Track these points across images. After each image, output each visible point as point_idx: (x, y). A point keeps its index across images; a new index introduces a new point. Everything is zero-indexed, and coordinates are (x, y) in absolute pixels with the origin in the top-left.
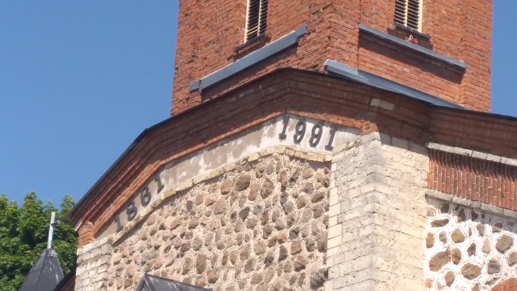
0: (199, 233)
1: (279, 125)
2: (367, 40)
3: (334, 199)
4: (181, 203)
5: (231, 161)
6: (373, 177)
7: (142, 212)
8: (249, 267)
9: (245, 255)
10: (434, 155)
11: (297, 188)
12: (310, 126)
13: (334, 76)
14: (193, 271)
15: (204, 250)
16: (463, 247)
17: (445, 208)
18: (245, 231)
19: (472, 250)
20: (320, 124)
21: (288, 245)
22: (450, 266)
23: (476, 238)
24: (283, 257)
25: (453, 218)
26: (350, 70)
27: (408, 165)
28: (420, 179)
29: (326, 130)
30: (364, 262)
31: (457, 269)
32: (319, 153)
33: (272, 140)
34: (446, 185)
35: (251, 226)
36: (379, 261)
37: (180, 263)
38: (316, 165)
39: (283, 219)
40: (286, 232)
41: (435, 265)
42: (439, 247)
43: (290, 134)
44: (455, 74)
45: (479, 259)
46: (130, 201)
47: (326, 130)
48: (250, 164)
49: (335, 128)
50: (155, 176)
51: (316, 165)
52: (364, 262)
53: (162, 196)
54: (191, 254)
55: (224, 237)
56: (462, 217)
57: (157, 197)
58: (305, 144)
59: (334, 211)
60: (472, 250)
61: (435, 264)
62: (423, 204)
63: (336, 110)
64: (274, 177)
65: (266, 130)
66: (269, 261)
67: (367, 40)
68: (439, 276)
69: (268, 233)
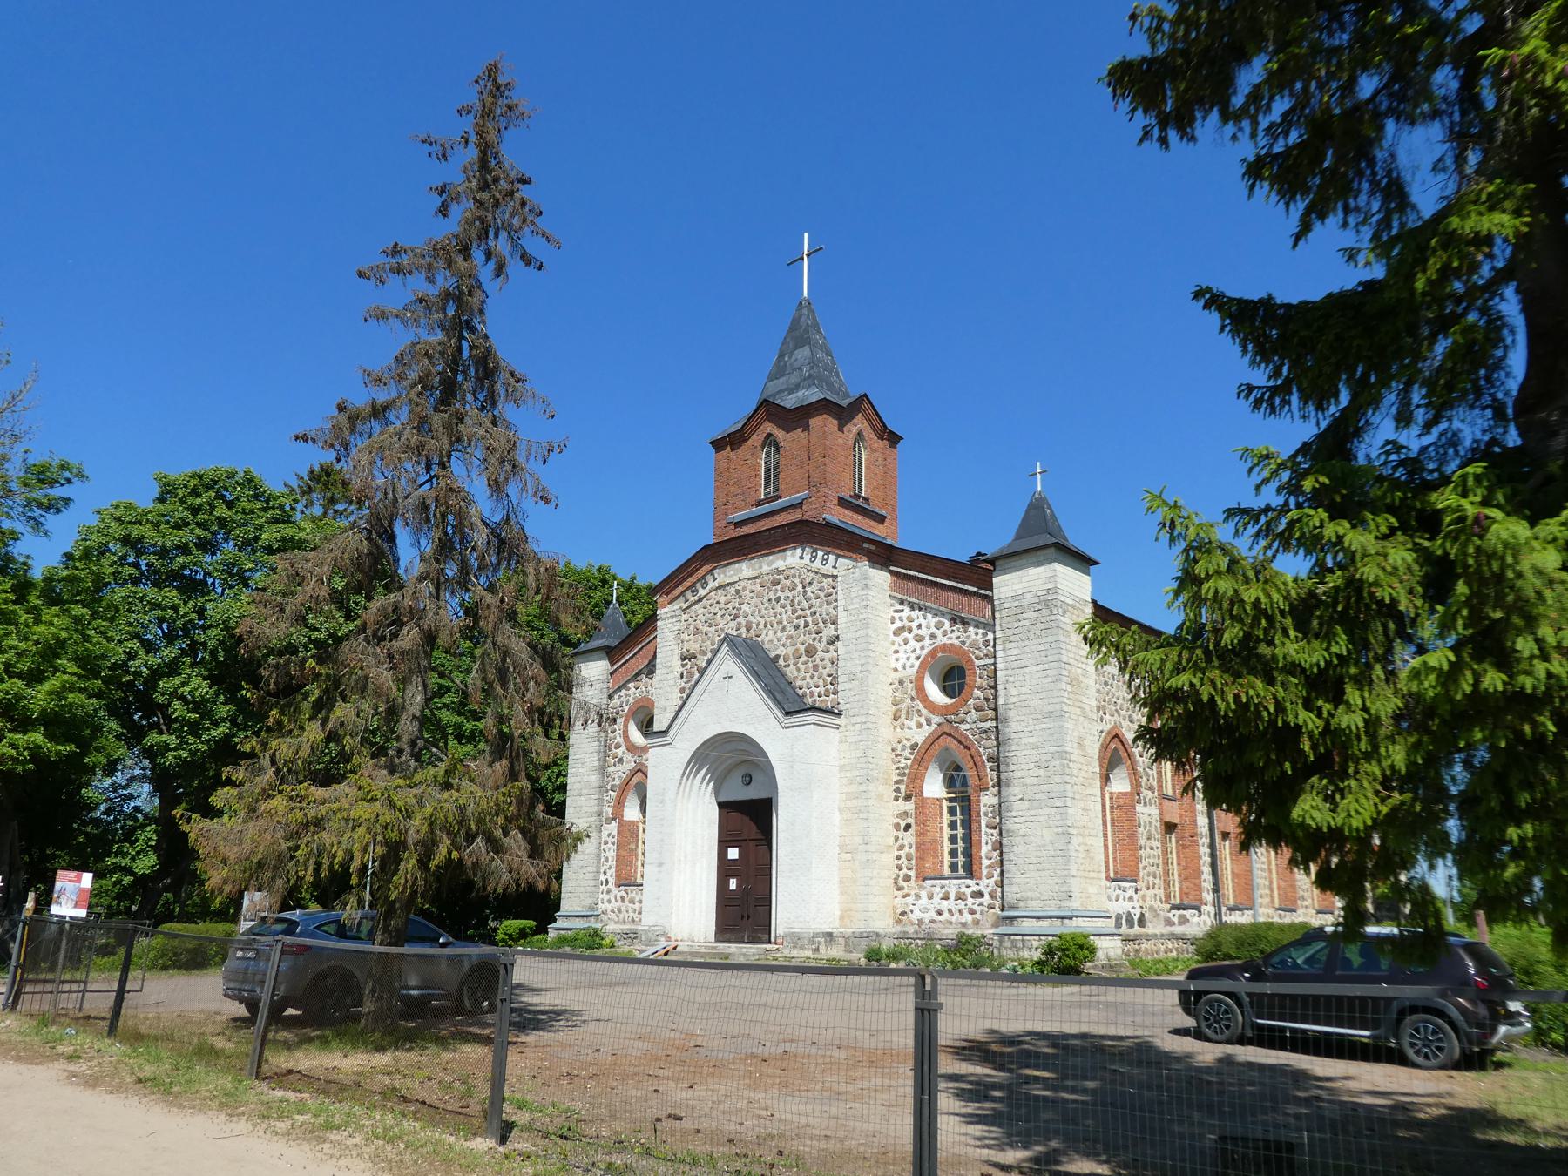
0: (745, 607)
1: (799, 551)
2: (842, 502)
3: (840, 596)
4: (732, 590)
5: (766, 569)
6: (866, 586)
7: (702, 592)
8: (783, 629)
9: (780, 623)
10: (891, 572)
11: (814, 587)
12: (820, 554)
13: (829, 525)
14: (743, 630)
15: (750, 618)
16: (914, 625)
17: (902, 603)
18: (779, 609)
19: (919, 626)
20: (828, 553)
21: (809, 619)
22: (906, 634)
23: (921, 620)
24: (807, 625)
25: (907, 609)
26: (834, 520)
27: (881, 579)
28: (887, 586)
29: (832, 557)
30: (862, 633)
31: (910, 636)
32: (828, 569)
33: (794, 559)
34: (902, 591)
35: (783, 607)
36: (871, 632)
37: (733, 624)
38: (826, 576)
39: (805, 605)
40: (808, 612)
41: (897, 633)
42: (898, 624)
43: (807, 557)
44: (881, 519)
45: (923, 632)
46: (693, 585)
47: (832, 557)
48: (781, 572)
49: (838, 556)
50: (711, 572)
51: (826, 576)
52: (862, 633)
53: (716, 584)
54: (740, 619)
55: (764, 612)
56: (913, 609)
57: (711, 585)
58: (817, 564)
59: (841, 603)
60: (919, 626)
61: (897, 633)
62: (889, 600)
63: (839, 547)
64: (797, 580)
65: (789, 553)
66: (797, 627)
67: (842, 502)
68: (899, 639)
69: (795, 611)
